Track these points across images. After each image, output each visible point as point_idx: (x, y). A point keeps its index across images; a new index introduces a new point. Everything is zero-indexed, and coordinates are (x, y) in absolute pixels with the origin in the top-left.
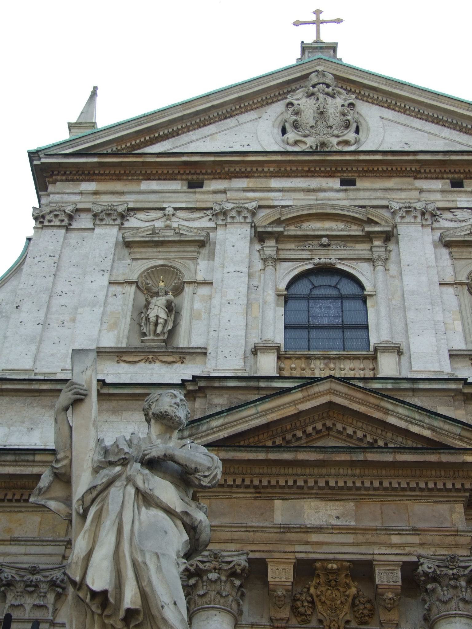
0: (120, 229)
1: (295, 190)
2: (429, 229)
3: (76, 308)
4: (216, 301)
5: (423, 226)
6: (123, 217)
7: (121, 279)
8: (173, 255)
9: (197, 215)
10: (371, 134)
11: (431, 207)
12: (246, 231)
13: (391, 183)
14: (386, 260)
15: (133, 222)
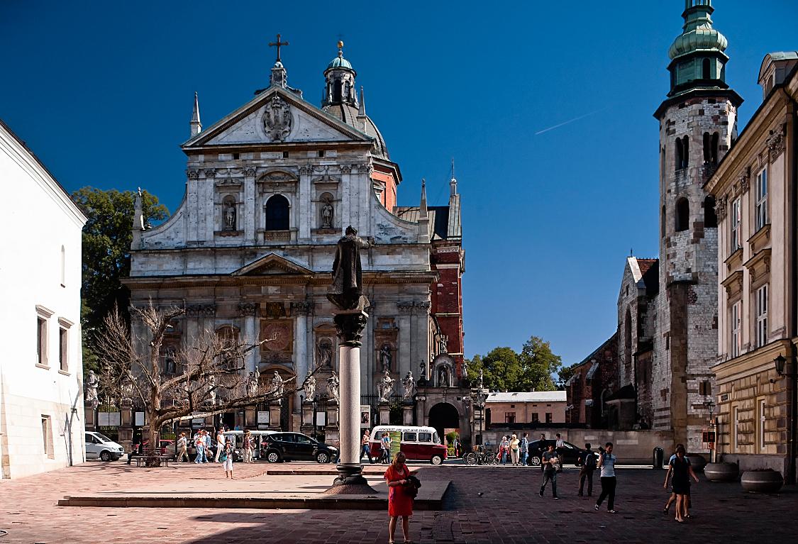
0: (215, 178)
1: (268, 159)
2: (309, 177)
3: (206, 215)
4: (245, 211)
5: (308, 176)
6: (214, 174)
7: (217, 202)
8: (232, 191)
9: (238, 171)
10: (295, 126)
11: (311, 167)
12: (253, 179)
13: (299, 155)
14: (295, 193)
15: (218, 175)
